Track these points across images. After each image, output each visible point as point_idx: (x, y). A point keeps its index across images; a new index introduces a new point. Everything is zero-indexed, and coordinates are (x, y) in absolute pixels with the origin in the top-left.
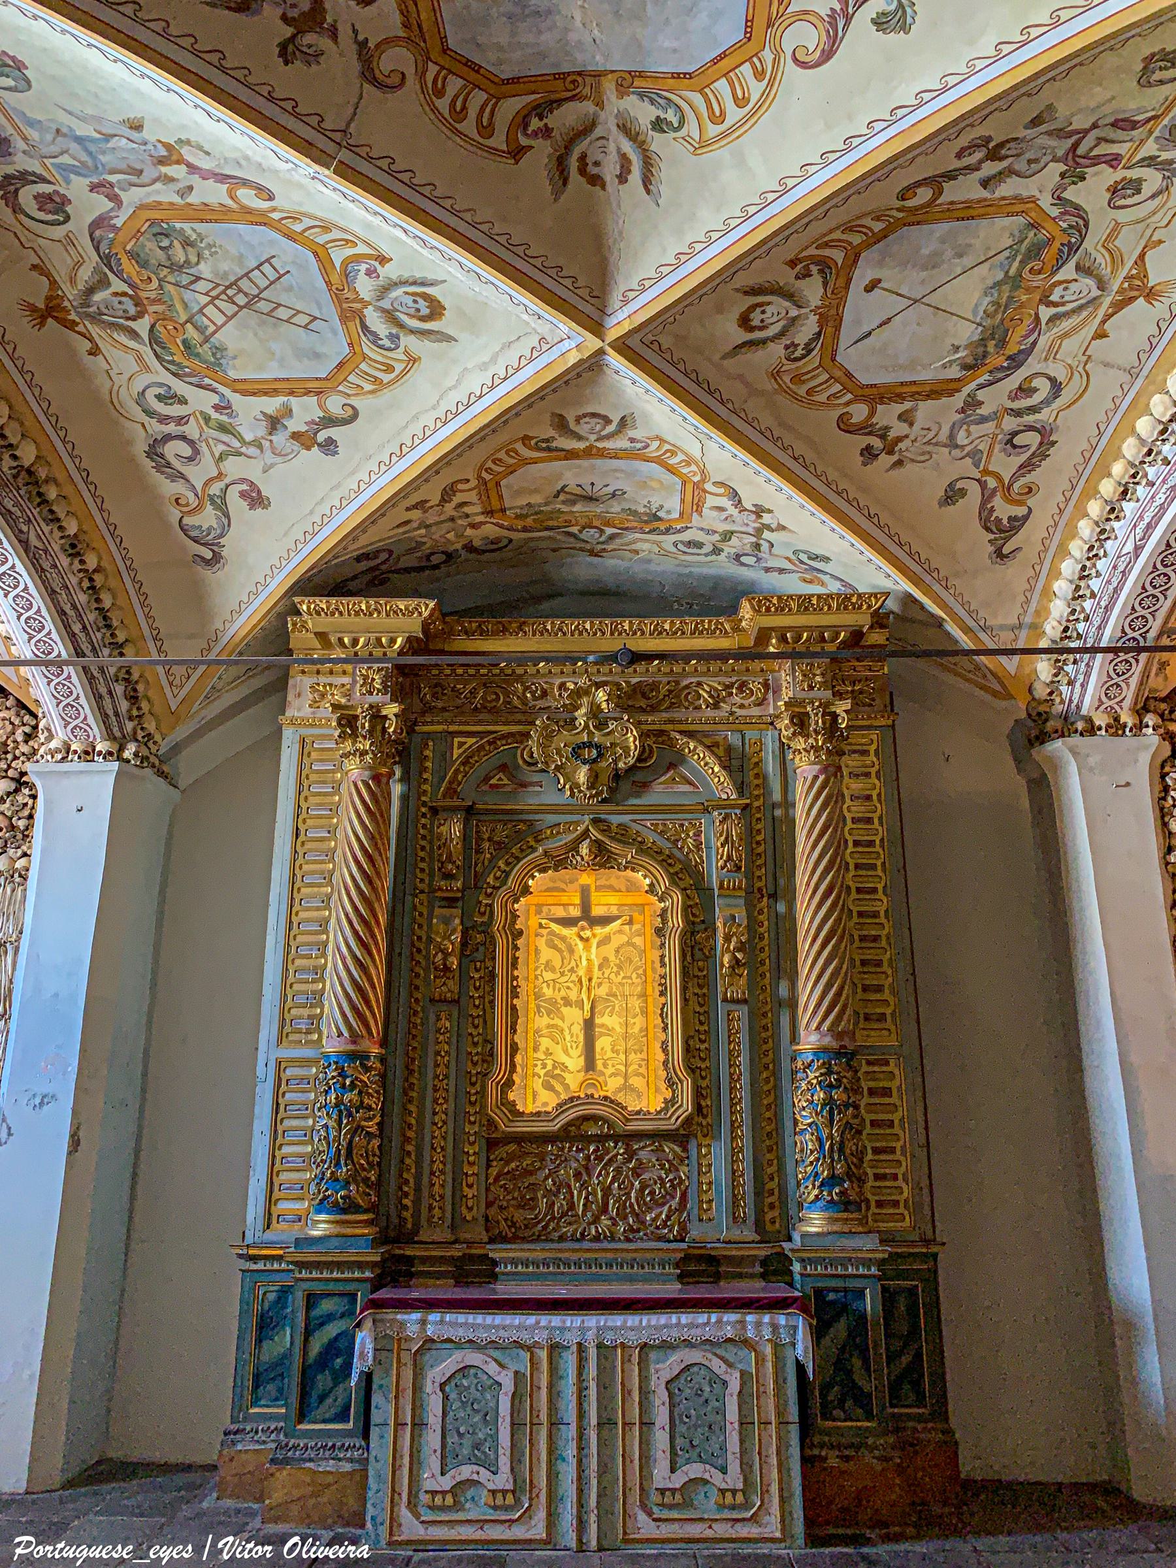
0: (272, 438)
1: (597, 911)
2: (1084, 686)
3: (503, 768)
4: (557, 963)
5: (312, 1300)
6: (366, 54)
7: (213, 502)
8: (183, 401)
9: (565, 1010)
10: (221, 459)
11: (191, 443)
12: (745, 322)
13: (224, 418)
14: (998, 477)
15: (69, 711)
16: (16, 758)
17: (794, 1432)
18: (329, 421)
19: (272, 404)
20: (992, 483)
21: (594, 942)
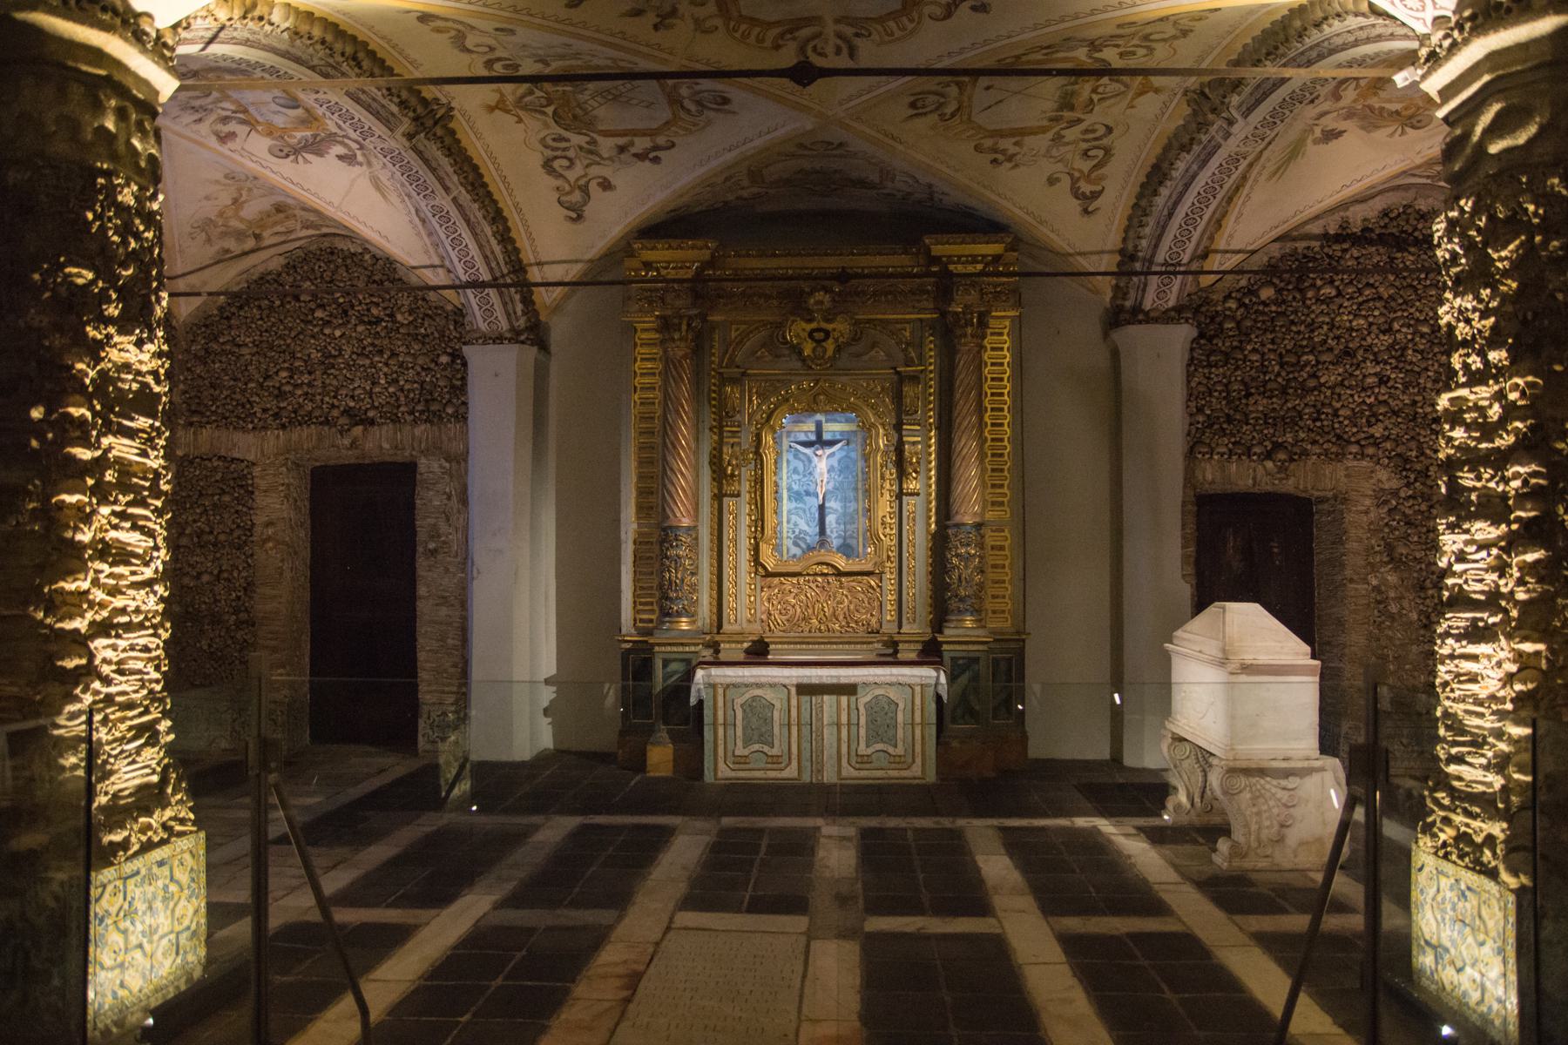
0: (622, 156)
1: (826, 437)
2: (1144, 290)
3: (763, 345)
4: (801, 468)
5: (666, 663)
6: (697, 22)
7: (579, 187)
8: (567, 140)
9: (806, 498)
10: (587, 166)
11: (570, 160)
12: (913, 105)
13: (592, 148)
14: (1080, 171)
15: (490, 311)
16: (450, 340)
17: (934, 729)
18: (656, 148)
19: (621, 141)
20: (1077, 174)
21: (825, 457)
